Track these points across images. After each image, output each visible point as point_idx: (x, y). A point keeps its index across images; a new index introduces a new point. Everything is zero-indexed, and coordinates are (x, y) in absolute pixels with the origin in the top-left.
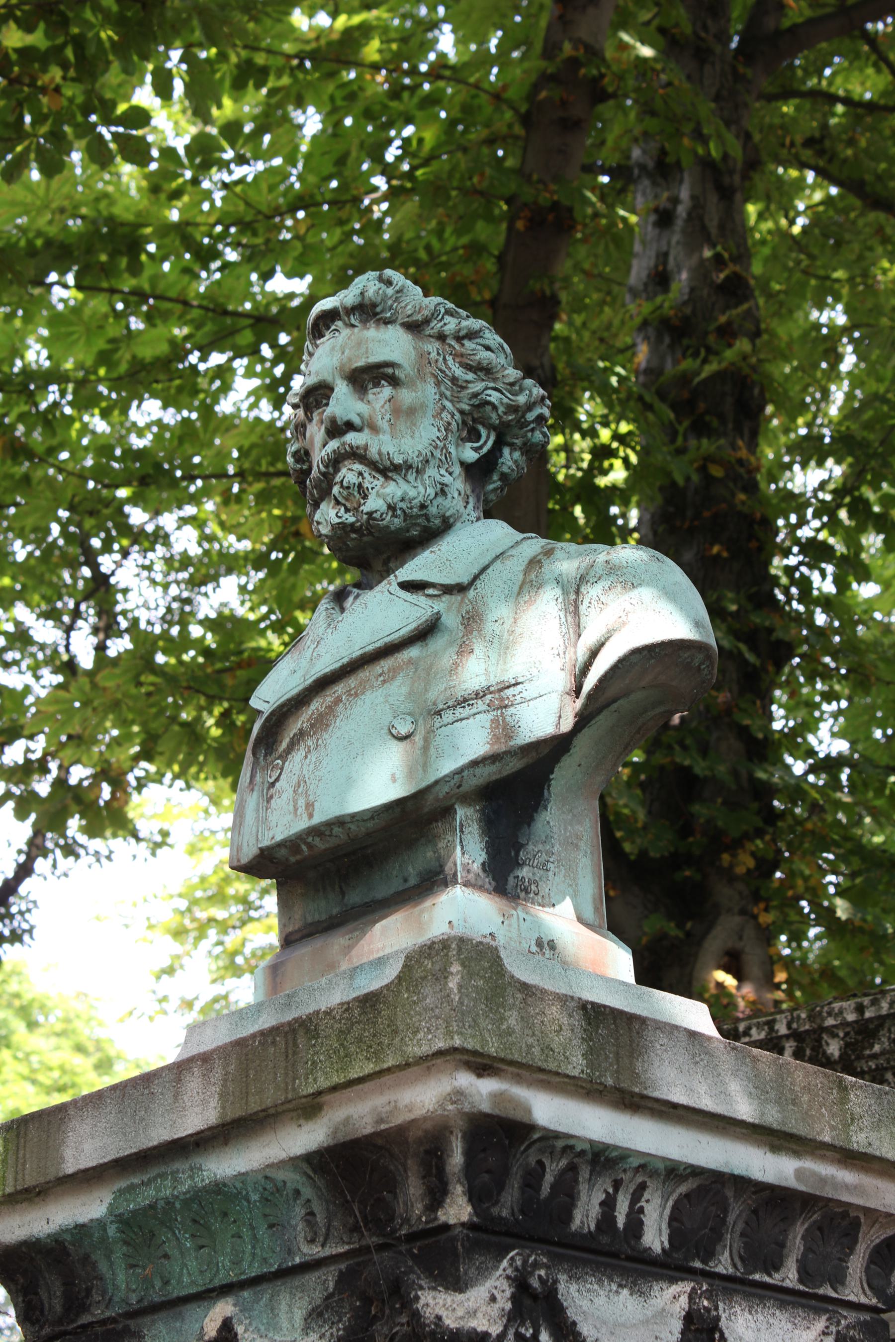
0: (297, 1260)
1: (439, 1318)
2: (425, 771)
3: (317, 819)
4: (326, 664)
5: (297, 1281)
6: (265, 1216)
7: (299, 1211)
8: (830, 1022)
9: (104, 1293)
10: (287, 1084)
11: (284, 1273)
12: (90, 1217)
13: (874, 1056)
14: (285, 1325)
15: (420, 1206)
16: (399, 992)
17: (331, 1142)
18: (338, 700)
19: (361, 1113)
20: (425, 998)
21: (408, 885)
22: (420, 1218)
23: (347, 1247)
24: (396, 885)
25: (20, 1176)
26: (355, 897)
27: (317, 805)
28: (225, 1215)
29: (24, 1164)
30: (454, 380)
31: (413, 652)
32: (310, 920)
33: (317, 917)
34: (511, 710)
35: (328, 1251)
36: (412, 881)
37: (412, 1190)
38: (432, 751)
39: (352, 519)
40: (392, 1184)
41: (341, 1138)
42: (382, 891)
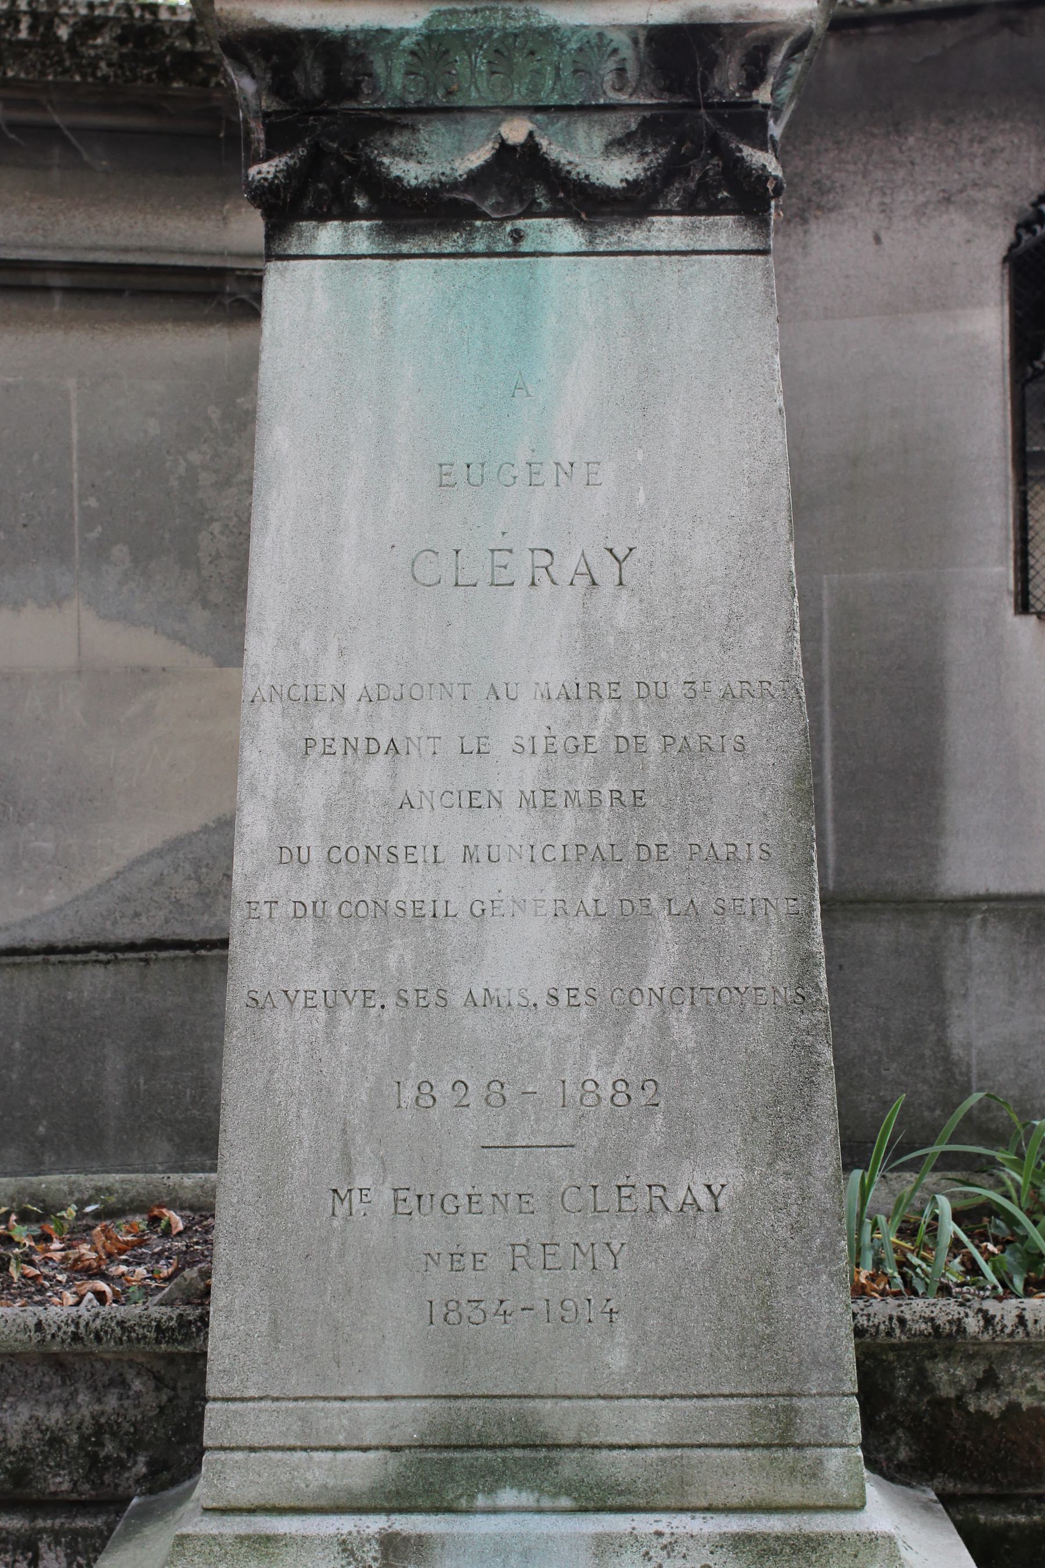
0: (602, 101)
1: (764, 166)
5: (596, 117)
6: (574, 61)
7: (611, 64)
8: (64, 10)
9: (375, 88)
11: (583, 109)
12: (401, 25)
13: (95, 47)
14: (583, 146)
15: (735, 84)
17: (686, 21)
22: (734, 93)
23: (654, 101)
28: (532, 53)
35: (634, 100)
37: (730, 72)
40: (713, 63)
41: (696, 20)
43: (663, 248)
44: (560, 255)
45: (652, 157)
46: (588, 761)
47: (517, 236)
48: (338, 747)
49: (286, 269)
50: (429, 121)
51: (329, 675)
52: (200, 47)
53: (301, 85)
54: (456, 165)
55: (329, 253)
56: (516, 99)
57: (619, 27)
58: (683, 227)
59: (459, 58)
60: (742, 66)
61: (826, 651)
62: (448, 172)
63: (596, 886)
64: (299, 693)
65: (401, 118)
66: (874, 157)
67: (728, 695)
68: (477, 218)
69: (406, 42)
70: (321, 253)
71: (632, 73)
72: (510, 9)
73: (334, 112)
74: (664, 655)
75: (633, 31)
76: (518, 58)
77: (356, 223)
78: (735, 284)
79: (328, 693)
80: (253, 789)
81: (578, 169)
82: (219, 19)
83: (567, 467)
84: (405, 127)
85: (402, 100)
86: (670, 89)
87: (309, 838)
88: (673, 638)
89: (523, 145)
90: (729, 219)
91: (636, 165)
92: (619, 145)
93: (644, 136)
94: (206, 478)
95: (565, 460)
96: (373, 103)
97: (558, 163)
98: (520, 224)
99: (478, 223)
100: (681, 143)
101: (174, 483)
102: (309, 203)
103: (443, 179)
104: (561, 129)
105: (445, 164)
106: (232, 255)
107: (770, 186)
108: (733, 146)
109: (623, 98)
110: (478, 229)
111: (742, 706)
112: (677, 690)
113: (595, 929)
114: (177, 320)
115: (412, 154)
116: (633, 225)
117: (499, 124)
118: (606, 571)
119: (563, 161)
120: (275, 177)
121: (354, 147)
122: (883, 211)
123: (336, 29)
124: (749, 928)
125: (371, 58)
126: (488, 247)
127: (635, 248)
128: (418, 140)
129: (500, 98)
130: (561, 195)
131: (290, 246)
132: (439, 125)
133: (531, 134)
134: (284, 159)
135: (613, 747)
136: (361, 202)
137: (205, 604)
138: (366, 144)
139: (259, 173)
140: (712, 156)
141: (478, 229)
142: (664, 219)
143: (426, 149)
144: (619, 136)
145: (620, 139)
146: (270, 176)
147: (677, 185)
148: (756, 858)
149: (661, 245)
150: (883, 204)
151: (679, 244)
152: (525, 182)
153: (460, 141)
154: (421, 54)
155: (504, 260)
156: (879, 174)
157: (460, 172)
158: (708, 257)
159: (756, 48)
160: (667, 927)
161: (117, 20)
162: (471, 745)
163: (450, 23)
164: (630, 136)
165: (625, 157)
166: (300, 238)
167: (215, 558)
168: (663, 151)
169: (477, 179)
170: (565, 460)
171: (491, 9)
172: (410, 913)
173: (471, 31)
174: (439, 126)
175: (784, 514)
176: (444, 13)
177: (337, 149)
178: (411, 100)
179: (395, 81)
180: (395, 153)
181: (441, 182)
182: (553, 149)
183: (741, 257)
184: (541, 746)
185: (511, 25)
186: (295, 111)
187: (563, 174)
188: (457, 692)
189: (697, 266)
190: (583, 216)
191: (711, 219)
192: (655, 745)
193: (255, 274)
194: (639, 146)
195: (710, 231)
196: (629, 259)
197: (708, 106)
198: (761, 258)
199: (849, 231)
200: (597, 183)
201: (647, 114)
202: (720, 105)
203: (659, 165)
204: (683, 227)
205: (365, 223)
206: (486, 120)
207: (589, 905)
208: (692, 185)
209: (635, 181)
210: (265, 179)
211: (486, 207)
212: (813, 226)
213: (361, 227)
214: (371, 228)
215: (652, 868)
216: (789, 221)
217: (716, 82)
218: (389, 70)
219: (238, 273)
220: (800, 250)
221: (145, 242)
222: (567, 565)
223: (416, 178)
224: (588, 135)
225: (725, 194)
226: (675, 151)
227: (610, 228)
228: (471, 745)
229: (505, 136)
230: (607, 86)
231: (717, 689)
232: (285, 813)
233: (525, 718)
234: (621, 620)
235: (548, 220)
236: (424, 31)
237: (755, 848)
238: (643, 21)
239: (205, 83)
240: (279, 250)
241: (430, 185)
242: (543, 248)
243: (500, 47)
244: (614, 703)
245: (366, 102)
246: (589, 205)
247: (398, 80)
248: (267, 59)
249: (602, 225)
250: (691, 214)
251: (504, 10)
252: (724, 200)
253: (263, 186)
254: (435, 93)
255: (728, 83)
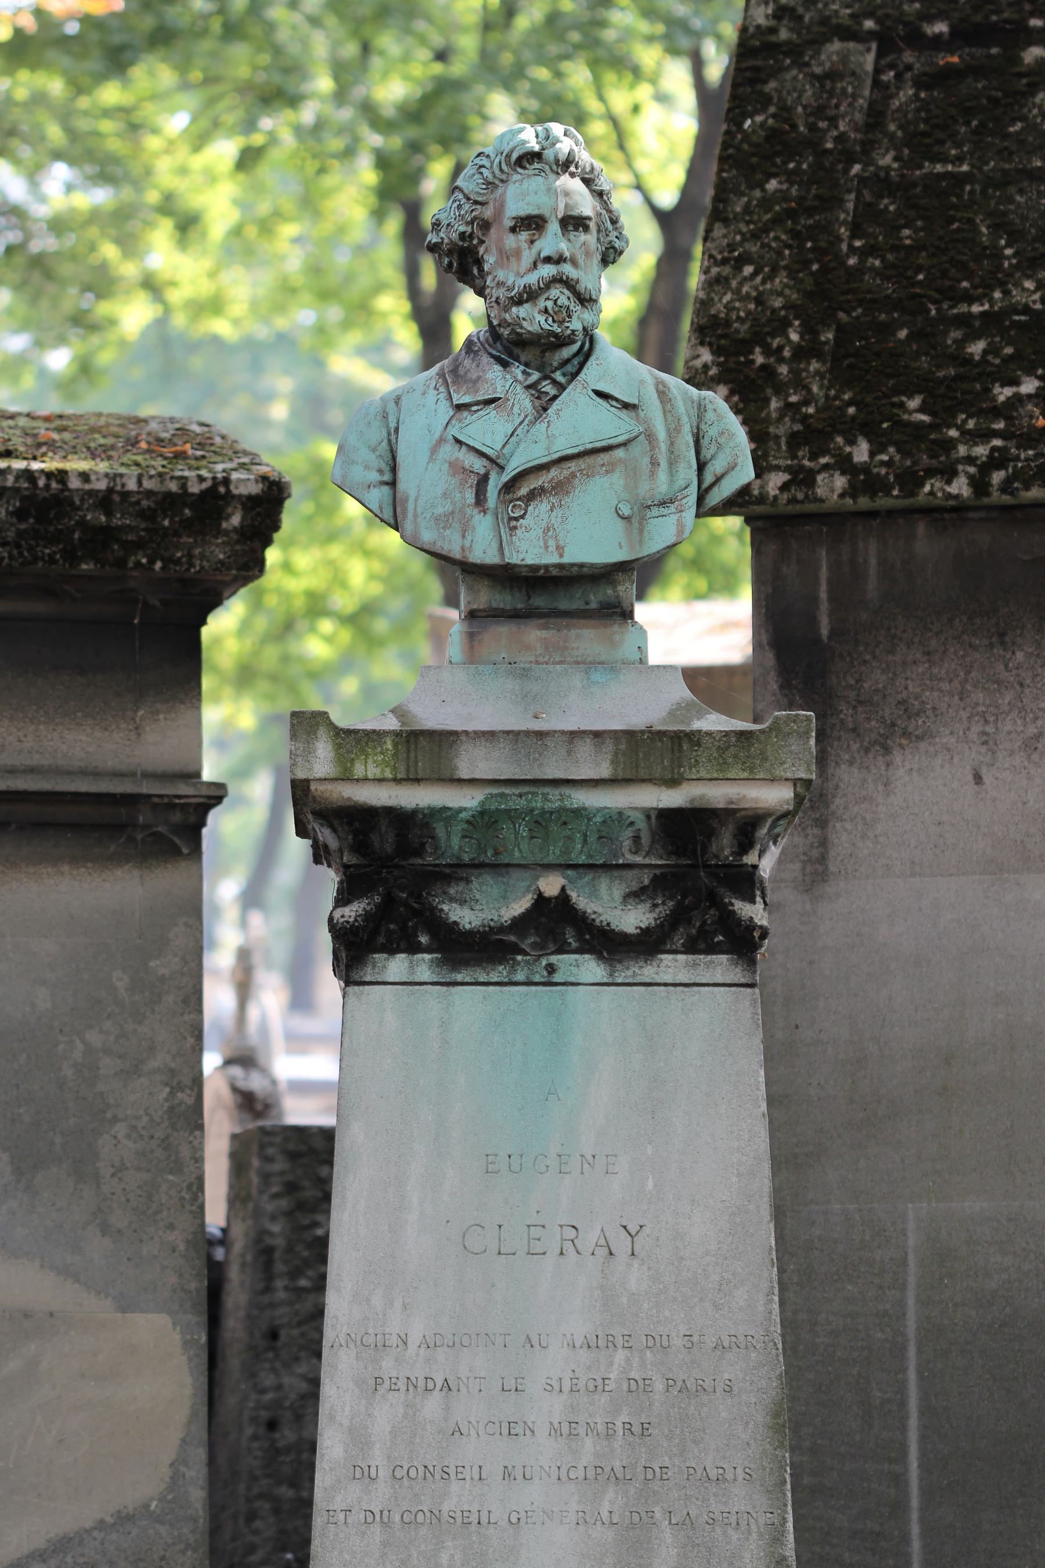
0: (621, 862)
1: (751, 918)
2: (641, 546)
3: (566, 560)
4: (563, 446)
5: (616, 873)
7: (629, 833)
9: (437, 848)
10: (673, 770)
11: (606, 867)
14: (605, 897)
16: (770, 737)
17: (688, 805)
18: (573, 475)
19: (717, 794)
20: (790, 746)
21: (588, 607)
22: (727, 858)
24: (576, 604)
25: (412, 769)
26: (540, 601)
27: (566, 549)
28: (565, 823)
29: (416, 762)
30: (606, 229)
31: (620, 453)
32: (495, 605)
33: (502, 606)
34: (684, 514)
35: (647, 861)
36: (594, 605)
37: (725, 841)
38: (646, 534)
39: (559, 330)
40: (711, 834)
41: (697, 805)
42: (564, 605)
43: (670, 981)
44: (586, 985)
45: (661, 908)
46: (604, 1399)
47: (551, 969)
48: (402, 1385)
49: (362, 993)
50: (480, 874)
51: (395, 1325)
52: (117, 520)
53: (377, 845)
54: (503, 912)
55: (397, 980)
56: (551, 859)
57: (636, 809)
58: (687, 964)
59: (506, 829)
60: (735, 836)
61: (911, 1301)
62: (496, 918)
63: (611, 1501)
64: (370, 1340)
65: (456, 873)
66: (973, 674)
67: (719, 1346)
68: (519, 954)
69: (463, 815)
70: (391, 980)
71: (645, 840)
72: (548, 794)
73: (403, 867)
74: (667, 1313)
75: (647, 813)
76: (554, 827)
77: (420, 956)
78: (728, 1011)
79: (394, 1341)
80: (332, 1418)
81: (601, 918)
82: (314, 797)
83: (590, 1159)
84: (462, 879)
85: (458, 858)
86: (677, 853)
87: (378, 1458)
88: (675, 1299)
89: (557, 898)
90: (724, 958)
91: (648, 915)
92: (635, 895)
93: (655, 890)
94: (108, 1065)
95: (588, 1153)
96: (435, 860)
97: (585, 912)
98: (554, 959)
99: (519, 958)
100: (684, 896)
101: (69, 1072)
102: (381, 940)
103: (492, 924)
104: (588, 883)
105: (493, 911)
106: (148, 775)
107: (756, 934)
108: (727, 900)
109: (638, 859)
110: (519, 963)
111: (730, 1356)
112: (678, 1342)
113: (610, 1534)
114: (75, 861)
115: (466, 901)
116: (646, 962)
117: (537, 878)
118: (621, 1244)
119: (589, 911)
120: (356, 920)
121: (420, 896)
122: (985, 743)
123: (408, 806)
124: (734, 1536)
125: (434, 825)
126: (527, 978)
127: (647, 980)
128: (471, 890)
129: (538, 857)
130: (587, 937)
131: (365, 974)
132: (488, 878)
133: (563, 889)
134: (362, 906)
135: (625, 1387)
136: (424, 939)
137: (105, 1229)
138: (429, 894)
139: (343, 916)
140: (710, 907)
141: (519, 963)
142: (670, 957)
143: (478, 897)
144: (635, 889)
145: (636, 892)
146: (352, 920)
147: (681, 930)
148: (740, 1479)
149: (668, 978)
150: (984, 733)
151: (683, 978)
152: (557, 925)
153: (506, 891)
154: (475, 823)
155: (540, 988)
156: (979, 696)
157: (506, 919)
158: (707, 988)
159: (745, 823)
160: (668, 1536)
161: (16, 490)
162: (510, 1384)
163: (500, 803)
164: (643, 890)
165: (639, 906)
166: (374, 967)
167: (119, 1170)
168: (671, 904)
169: (519, 924)
170: (588, 1153)
171: (533, 793)
172: (459, 1520)
173: (516, 810)
174: (488, 878)
175: (766, 1199)
176: (496, 795)
177: (407, 898)
178: (466, 858)
179: (454, 844)
180: (452, 900)
181: (490, 927)
182: (581, 901)
183: (733, 989)
184: (567, 1386)
185: (548, 806)
186: (371, 866)
187: (589, 921)
188: (499, 1341)
189: (697, 996)
190: (605, 954)
191: (709, 957)
192: (659, 1386)
193: (177, 801)
194: (651, 898)
195: (708, 967)
196: (642, 989)
197: (706, 866)
198: (749, 990)
199: (942, 767)
200: (617, 929)
201: (658, 872)
202: (717, 866)
203: (667, 915)
204: (687, 964)
205: (427, 957)
206: (527, 874)
207: (605, 1515)
208: (694, 931)
209: (648, 929)
210: (348, 922)
211: (525, 945)
212: (897, 757)
213: (423, 959)
214: (432, 961)
215: (656, 1485)
216: (867, 750)
217: (714, 848)
218: (449, 834)
219: (155, 800)
220: (881, 787)
221: (36, 760)
222: (590, 1238)
223: (470, 923)
224: (610, 889)
225: (721, 938)
226: (679, 904)
227: (626, 964)
228: (510, 1384)
229: (542, 890)
230: (625, 850)
231: (710, 1341)
232: (359, 1438)
233: (555, 1362)
234: (632, 1285)
235: (576, 956)
236: (479, 809)
237: (739, 1471)
238: (655, 805)
239: (121, 563)
240: (356, 978)
241: (481, 929)
242: (572, 979)
243: (540, 820)
244: (626, 1351)
245: (430, 859)
246: (608, 945)
247: (456, 842)
248: (350, 824)
249: (620, 961)
250: (693, 953)
251: (543, 794)
252: (720, 943)
253: (345, 927)
254: (486, 852)
255: (722, 849)
